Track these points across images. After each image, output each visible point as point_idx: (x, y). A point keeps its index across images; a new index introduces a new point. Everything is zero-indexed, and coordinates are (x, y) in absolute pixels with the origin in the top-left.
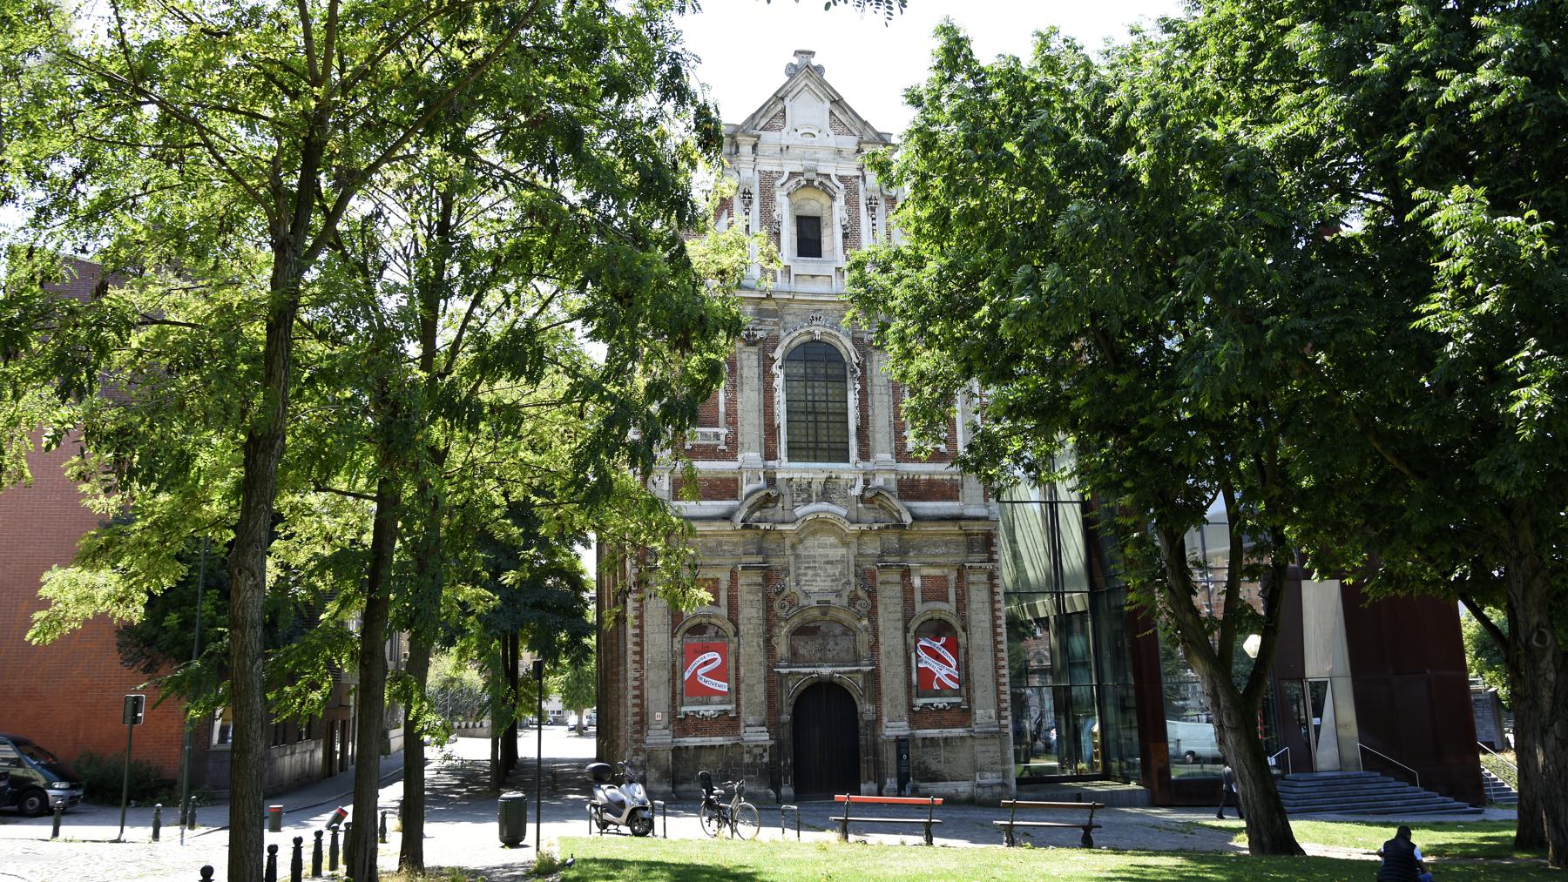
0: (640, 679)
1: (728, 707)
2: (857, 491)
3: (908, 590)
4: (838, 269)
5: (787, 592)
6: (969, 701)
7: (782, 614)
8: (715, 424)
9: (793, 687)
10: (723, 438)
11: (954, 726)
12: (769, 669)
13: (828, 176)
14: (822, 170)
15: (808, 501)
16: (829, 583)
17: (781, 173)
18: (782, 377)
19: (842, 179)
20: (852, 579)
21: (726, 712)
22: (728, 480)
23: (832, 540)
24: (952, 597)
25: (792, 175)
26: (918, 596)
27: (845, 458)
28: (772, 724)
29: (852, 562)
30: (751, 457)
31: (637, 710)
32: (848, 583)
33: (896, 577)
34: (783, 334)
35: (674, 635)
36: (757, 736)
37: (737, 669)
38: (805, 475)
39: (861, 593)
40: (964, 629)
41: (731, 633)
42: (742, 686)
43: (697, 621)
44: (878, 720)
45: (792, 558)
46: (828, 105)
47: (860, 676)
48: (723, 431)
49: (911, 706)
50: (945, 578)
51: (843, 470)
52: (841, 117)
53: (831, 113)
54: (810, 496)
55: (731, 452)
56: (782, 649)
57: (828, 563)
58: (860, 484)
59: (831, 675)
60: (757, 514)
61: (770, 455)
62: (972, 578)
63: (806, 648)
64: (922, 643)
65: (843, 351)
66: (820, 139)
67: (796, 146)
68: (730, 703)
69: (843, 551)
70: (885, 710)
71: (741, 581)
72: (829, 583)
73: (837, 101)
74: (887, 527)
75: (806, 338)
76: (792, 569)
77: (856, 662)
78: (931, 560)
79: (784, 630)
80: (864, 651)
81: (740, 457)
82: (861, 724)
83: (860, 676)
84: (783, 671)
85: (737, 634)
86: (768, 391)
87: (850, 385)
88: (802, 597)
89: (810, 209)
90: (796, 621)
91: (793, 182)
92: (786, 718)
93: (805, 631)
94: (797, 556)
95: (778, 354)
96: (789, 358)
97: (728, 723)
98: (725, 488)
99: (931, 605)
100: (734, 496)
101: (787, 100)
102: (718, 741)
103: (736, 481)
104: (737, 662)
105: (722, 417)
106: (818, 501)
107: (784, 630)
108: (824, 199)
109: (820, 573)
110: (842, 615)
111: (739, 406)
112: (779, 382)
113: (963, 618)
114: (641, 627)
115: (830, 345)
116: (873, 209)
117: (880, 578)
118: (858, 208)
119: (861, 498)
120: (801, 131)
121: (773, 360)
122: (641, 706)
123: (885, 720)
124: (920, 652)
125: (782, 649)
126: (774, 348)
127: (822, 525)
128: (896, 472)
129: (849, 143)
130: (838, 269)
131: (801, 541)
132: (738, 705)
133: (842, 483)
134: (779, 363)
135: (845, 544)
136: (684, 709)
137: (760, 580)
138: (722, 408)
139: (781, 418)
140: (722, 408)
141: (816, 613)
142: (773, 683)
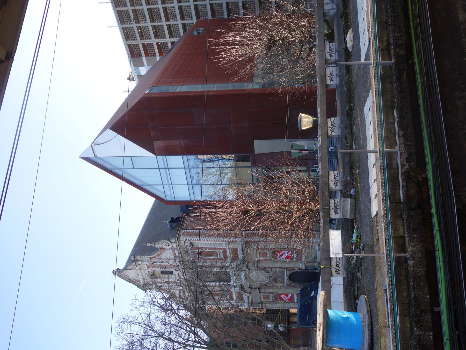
26: (266, 258)
50: (260, 253)
57: (257, 275)
64: (278, 258)
79: (275, 284)
80: (281, 270)
99: (268, 256)
110: (271, 274)
124: (281, 258)
125: (281, 285)
142: (288, 286)
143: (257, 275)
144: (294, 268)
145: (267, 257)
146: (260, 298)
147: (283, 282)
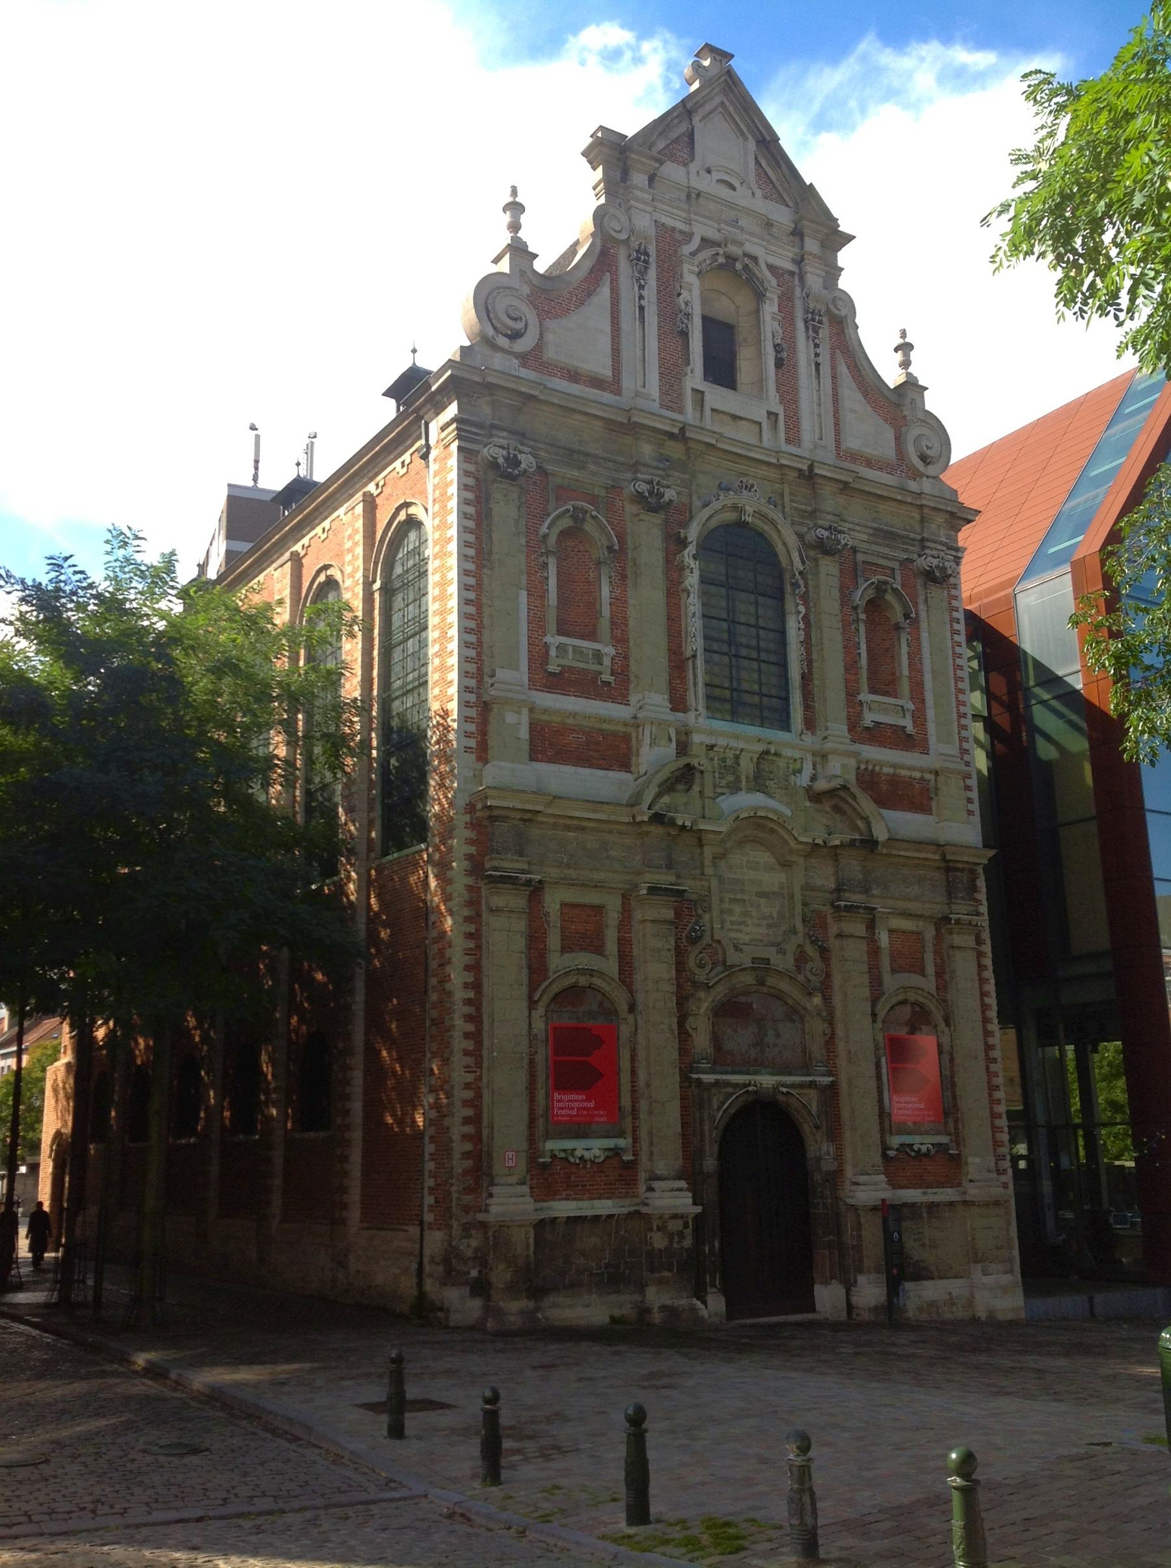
0: (475, 1086)
1: (622, 1143)
2: (804, 780)
3: (874, 951)
4: (769, 413)
5: (707, 940)
6: (958, 1140)
7: (701, 975)
8: (592, 636)
9: (720, 1108)
10: (607, 661)
11: (941, 1185)
12: (685, 1078)
13: (755, 259)
14: (750, 248)
15: (735, 788)
16: (764, 930)
17: (689, 236)
18: (697, 573)
19: (771, 267)
20: (800, 926)
21: (616, 1152)
22: (615, 734)
23: (764, 857)
24: (930, 969)
25: (706, 242)
26: (886, 963)
27: (786, 726)
28: (691, 1174)
29: (798, 897)
30: (651, 699)
31: (468, 1146)
32: (794, 931)
33: (860, 929)
34: (697, 503)
35: (532, 1004)
36: (673, 1200)
37: (634, 1072)
38: (733, 743)
39: (811, 951)
40: (948, 1024)
41: (623, 1007)
42: (643, 1105)
43: (571, 980)
44: (839, 1172)
45: (714, 883)
46: (752, 145)
47: (813, 1093)
48: (609, 650)
49: (885, 1148)
50: (919, 936)
54: (738, 779)
55: (618, 688)
56: (701, 1041)
57: (762, 895)
58: (808, 770)
59: (776, 1088)
60: (666, 799)
61: (678, 704)
62: (957, 940)
63: (740, 1039)
65: (780, 549)
66: (742, 197)
68: (621, 1134)
69: (780, 877)
70: (848, 1154)
71: (638, 915)
72: (764, 930)
74: (852, 843)
75: (731, 516)
76: (715, 899)
77: (806, 1067)
78: (902, 905)
79: (703, 1005)
80: (817, 1050)
81: (634, 698)
82: (817, 1177)
83: (813, 1093)
84: (708, 1078)
85: (632, 1008)
86: (674, 592)
87: (789, 605)
88: (730, 951)
89: (724, 309)
90: (720, 992)
91: (706, 254)
92: (710, 1164)
93: (731, 1010)
94: (721, 879)
95: (693, 533)
96: (706, 547)
97: (621, 1173)
98: (610, 750)
100: (624, 764)
101: (696, 119)
102: (604, 1207)
103: (627, 738)
104: (633, 1059)
105: (604, 624)
106: (750, 790)
107: (703, 1005)
108: (744, 300)
109: (753, 907)
110: (784, 986)
111: (632, 613)
112: (692, 580)
113: (943, 1002)
114: (477, 986)
116: (816, 331)
117: (833, 929)
119: (808, 789)
120: (716, 176)
121: (683, 543)
122: (476, 1138)
123: (849, 1171)
125: (701, 1041)
126: (685, 524)
127: (758, 829)
128: (856, 754)
130: (769, 413)
131: (723, 856)
132: (635, 1140)
133: (781, 763)
134: (691, 549)
135: (786, 865)
136: (550, 1145)
137: (670, 914)
138: (606, 612)
139: (695, 643)
140: (606, 612)
141: (748, 979)
142: (693, 1096)
143: (762, 895)
144: (834, 1132)
145: (894, 971)
146: (571, 883)
147: (721, 1058)
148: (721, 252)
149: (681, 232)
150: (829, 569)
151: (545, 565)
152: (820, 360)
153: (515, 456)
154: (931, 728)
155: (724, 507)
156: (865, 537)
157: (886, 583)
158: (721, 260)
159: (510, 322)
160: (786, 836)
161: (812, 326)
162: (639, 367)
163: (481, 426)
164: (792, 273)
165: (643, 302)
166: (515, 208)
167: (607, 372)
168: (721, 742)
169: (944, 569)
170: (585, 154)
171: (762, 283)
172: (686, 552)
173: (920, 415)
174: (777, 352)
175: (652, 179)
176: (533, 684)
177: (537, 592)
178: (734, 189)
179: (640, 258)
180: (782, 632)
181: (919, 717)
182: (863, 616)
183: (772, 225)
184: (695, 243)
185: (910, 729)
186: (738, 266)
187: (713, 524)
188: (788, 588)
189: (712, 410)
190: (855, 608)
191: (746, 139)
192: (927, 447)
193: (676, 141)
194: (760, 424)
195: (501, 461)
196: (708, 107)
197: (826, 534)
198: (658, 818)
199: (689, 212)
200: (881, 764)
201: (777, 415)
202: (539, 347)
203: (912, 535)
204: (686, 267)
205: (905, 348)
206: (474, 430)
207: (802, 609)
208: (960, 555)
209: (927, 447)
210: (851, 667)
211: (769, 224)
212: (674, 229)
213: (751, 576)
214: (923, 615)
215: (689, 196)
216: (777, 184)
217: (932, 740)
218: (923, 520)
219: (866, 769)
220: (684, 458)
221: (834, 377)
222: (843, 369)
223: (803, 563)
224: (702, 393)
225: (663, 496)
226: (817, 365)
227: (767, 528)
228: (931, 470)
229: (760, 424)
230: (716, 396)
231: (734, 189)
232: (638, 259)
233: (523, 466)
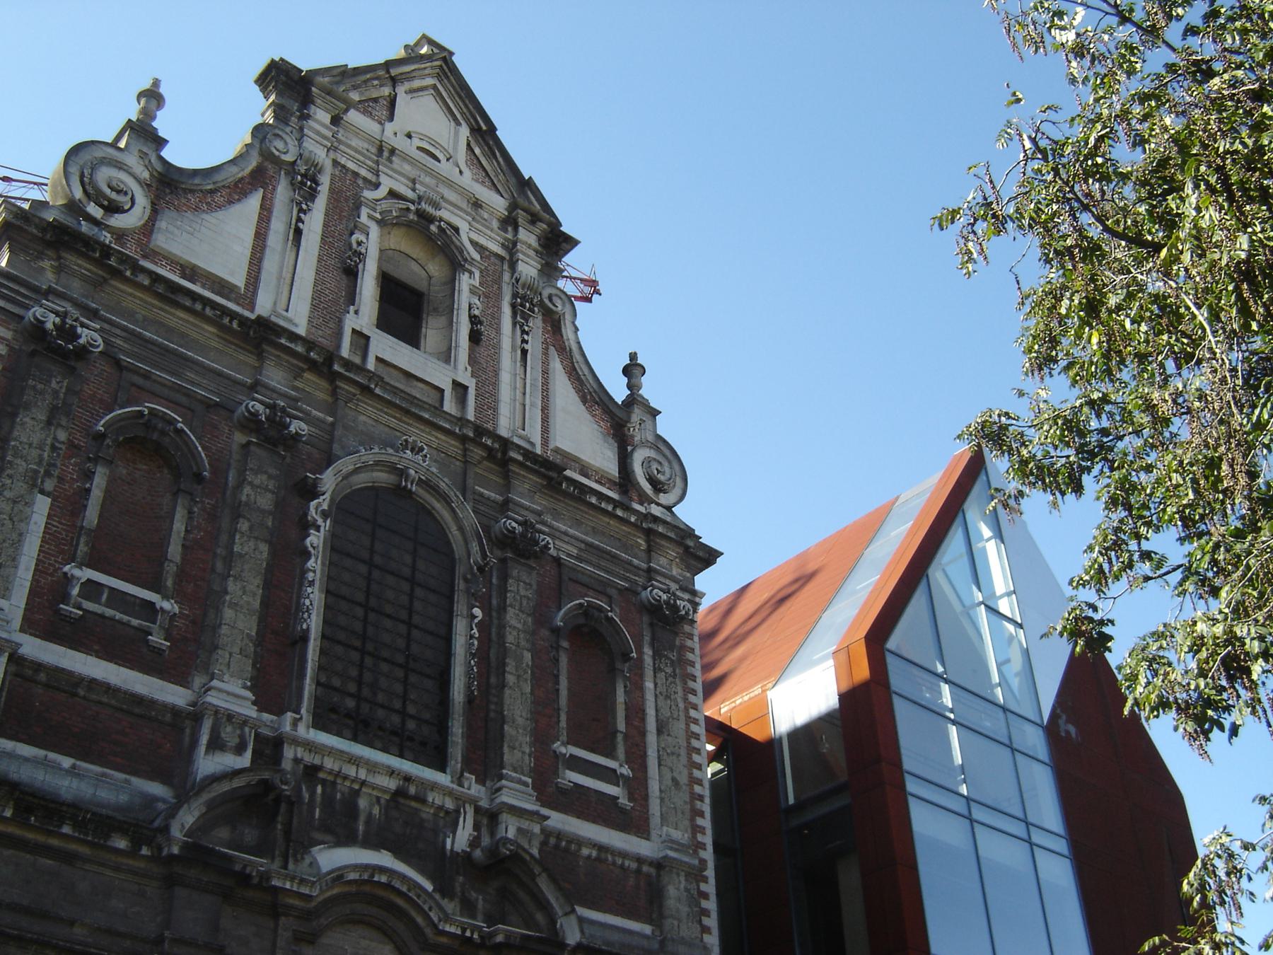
4: (456, 384)
13: (457, 230)
15: (347, 838)
25: (393, 194)
38: (351, 771)
46: (465, 131)
51: (434, 786)
52: (484, 162)
53: (468, 145)
66: (445, 168)
67: (406, 158)
73: (485, 134)
87: (460, 606)
101: (401, 90)
108: (436, 269)
115: (429, 513)
118: (499, 308)
120: (416, 142)
129: (498, 203)
130: (456, 384)
134: (324, 502)
138: (174, 551)
148: (412, 208)
149: (365, 179)
150: (522, 587)
151: (89, 476)
152: (526, 347)
153: (73, 328)
154: (655, 807)
155: (377, 463)
156: (575, 551)
157: (600, 609)
158: (411, 216)
159: (108, 191)
160: (419, 920)
161: (521, 310)
162: (286, 289)
163: (36, 290)
164: (502, 259)
165: (300, 225)
166: (152, 97)
167: (239, 280)
168: (329, 763)
169: (675, 609)
170: (256, 82)
171: (461, 252)
172: (313, 504)
173: (651, 438)
174: (472, 323)
175: (336, 120)
176: (29, 625)
177: (69, 506)
178: (439, 161)
179: (306, 184)
180: (448, 639)
181: (637, 786)
182: (565, 644)
183: (481, 207)
184: (382, 192)
185: (623, 801)
186: (433, 228)
187: (361, 480)
188: (460, 585)
189: (378, 358)
190: (556, 631)
191: (458, 124)
192: (658, 472)
193: (375, 100)
194: (442, 391)
195: (49, 326)
196: (417, 84)
197: (519, 529)
198: (196, 852)
199: (377, 163)
200: (580, 842)
201: (466, 388)
202: (148, 228)
203: (635, 561)
204: (364, 212)
205: (633, 370)
206: (22, 290)
207: (477, 611)
208: (697, 600)
209: (658, 472)
210: (543, 707)
211: (477, 204)
212: (356, 174)
213: (408, 559)
214: (648, 660)
215: (380, 150)
216: (492, 174)
217: (655, 820)
218: (649, 550)
219: (557, 847)
220: (330, 399)
221: (545, 372)
222: (557, 365)
223: (484, 556)
224: (367, 338)
225: (287, 426)
226: (524, 352)
227: (437, 505)
228: (664, 499)
229: (442, 391)
230: (385, 347)
231: (439, 161)
232: (303, 183)
233: (82, 341)
